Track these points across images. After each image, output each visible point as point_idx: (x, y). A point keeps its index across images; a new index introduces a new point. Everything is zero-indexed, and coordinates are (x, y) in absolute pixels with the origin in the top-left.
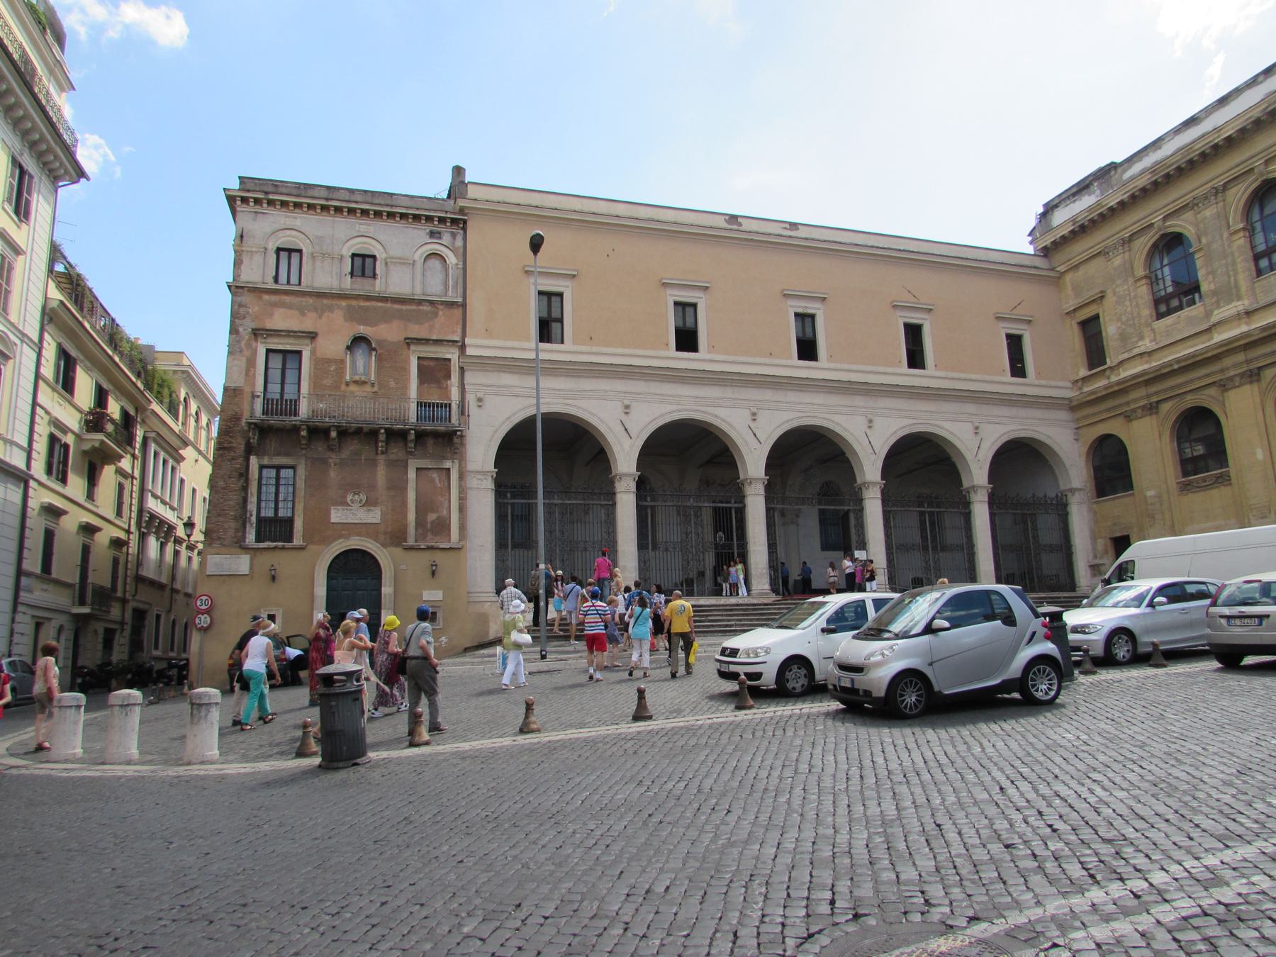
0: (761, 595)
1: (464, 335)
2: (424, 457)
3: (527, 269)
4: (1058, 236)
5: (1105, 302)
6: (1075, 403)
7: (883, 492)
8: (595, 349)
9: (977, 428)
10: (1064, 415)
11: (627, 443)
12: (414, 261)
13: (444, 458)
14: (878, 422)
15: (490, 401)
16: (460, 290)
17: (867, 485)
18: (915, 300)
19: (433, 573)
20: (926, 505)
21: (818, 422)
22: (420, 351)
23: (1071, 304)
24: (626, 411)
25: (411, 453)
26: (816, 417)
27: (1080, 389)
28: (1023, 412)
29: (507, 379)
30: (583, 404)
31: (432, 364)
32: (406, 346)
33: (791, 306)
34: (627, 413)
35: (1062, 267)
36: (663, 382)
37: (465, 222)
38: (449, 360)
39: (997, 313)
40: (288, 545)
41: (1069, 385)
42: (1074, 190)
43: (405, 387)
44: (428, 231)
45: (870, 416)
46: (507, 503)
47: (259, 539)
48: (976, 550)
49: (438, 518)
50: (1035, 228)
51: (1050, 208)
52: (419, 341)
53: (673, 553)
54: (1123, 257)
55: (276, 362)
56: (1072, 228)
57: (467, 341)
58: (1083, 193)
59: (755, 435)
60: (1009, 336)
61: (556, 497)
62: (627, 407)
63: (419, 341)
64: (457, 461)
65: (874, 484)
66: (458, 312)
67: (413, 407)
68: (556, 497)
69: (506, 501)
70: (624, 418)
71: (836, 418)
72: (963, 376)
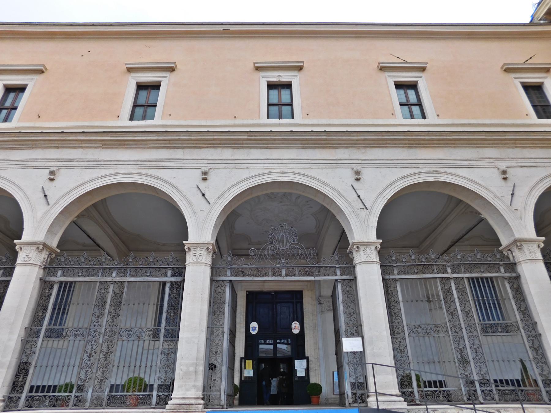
7: (381, 253)
20: (449, 270)
36: (103, 148)
39: (505, 65)
45: (355, 168)
48: (540, 330)
53: (72, 342)
59: (203, 195)
62: (52, 173)
65: (367, 244)
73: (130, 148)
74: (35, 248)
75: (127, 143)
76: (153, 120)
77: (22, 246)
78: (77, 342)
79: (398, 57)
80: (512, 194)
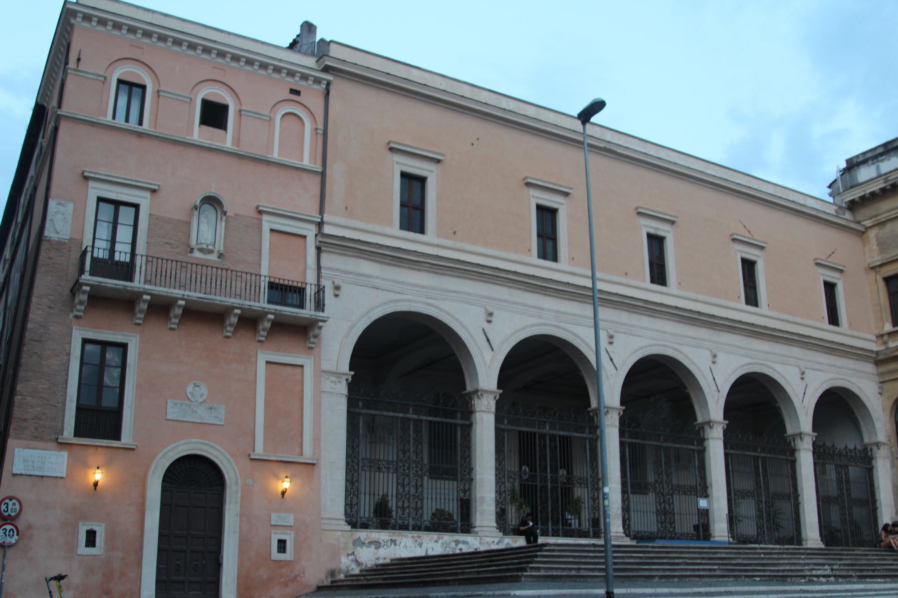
1: (321, 211)
3: (392, 145)
4: (868, 192)
6: (881, 357)
7: (725, 432)
8: (459, 245)
9: (803, 373)
10: (870, 368)
11: (488, 355)
14: (721, 358)
15: (345, 289)
17: (709, 423)
18: (748, 235)
20: (759, 450)
21: (669, 352)
22: (274, 223)
23: (877, 258)
26: (666, 346)
27: (885, 343)
29: (367, 267)
30: (446, 305)
33: (645, 226)
34: (489, 322)
35: (868, 222)
40: (115, 443)
41: (874, 338)
42: (881, 150)
46: (359, 414)
47: (77, 434)
50: (835, 181)
51: (853, 165)
55: (107, 211)
56: (884, 185)
57: (326, 218)
58: (892, 154)
59: (611, 360)
61: (411, 410)
68: (411, 410)
69: (357, 410)
70: (487, 326)
71: (685, 349)
72: (791, 318)
75: (548, 290)
77: (483, 393)
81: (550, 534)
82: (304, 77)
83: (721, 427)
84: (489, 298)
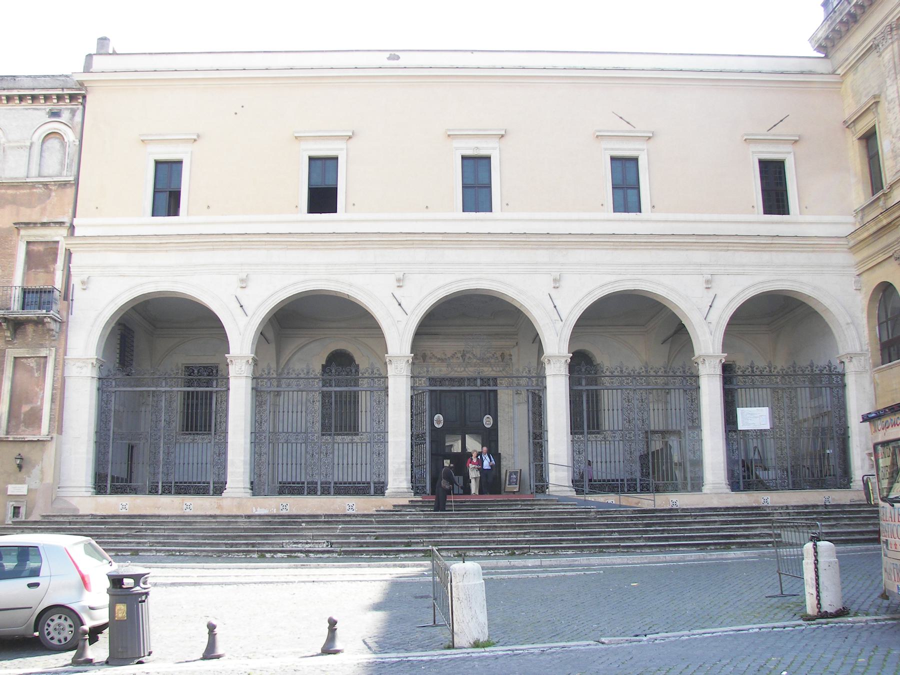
0: (396, 495)
1: (74, 216)
2: (28, 346)
5: (880, 109)
11: (242, 320)
12: (32, 144)
13: (42, 346)
16: (75, 169)
19: (20, 467)
24: (244, 285)
25: (8, 342)
28: (778, 258)
31: (41, 248)
32: (16, 231)
36: (288, 249)
37: (84, 97)
38: (58, 242)
43: (11, 275)
44: (48, 110)
49: (32, 409)
52: (27, 224)
54: (893, 50)
59: (400, 305)
60: (765, 165)
63: (27, 224)
64: (54, 349)
65: (559, 357)
66: (70, 191)
67: (17, 293)
70: (240, 293)
73: (318, 249)
74: (245, 361)
76: (336, 212)
78: (299, 445)
79: (621, 118)
80: (711, 306)
81: (319, 493)
82: (60, 98)
83: (563, 361)
84: (242, 264)
